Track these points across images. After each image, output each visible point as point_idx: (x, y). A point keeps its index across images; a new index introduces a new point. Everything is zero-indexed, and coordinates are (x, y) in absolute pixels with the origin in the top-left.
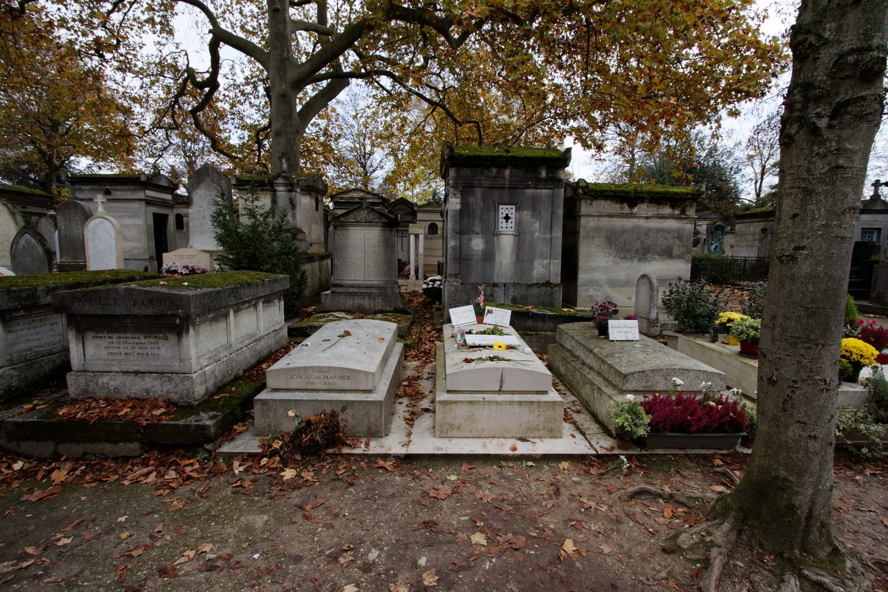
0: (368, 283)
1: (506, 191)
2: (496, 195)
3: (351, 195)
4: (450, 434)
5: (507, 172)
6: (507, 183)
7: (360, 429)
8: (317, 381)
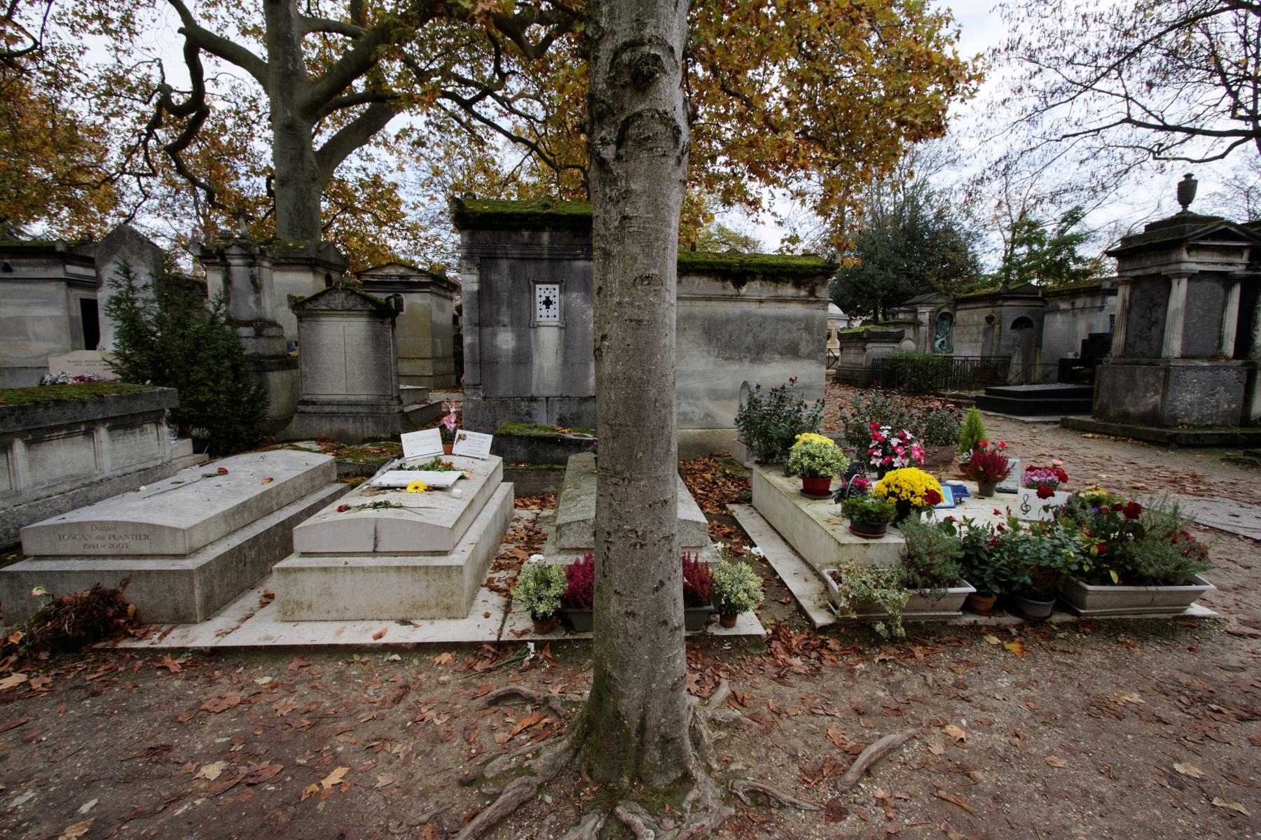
0: (352, 398)
1: (545, 263)
2: (531, 269)
3: (387, 271)
4: (297, 616)
5: (545, 237)
6: (546, 252)
7: (162, 611)
8: (100, 543)
